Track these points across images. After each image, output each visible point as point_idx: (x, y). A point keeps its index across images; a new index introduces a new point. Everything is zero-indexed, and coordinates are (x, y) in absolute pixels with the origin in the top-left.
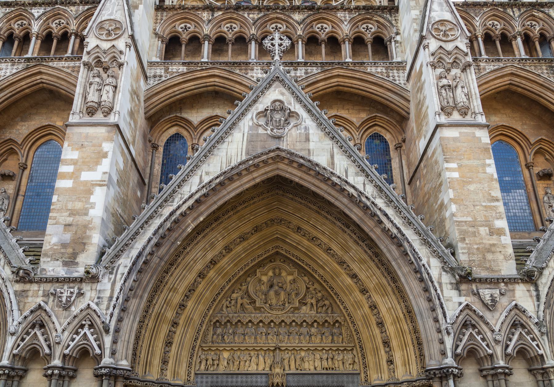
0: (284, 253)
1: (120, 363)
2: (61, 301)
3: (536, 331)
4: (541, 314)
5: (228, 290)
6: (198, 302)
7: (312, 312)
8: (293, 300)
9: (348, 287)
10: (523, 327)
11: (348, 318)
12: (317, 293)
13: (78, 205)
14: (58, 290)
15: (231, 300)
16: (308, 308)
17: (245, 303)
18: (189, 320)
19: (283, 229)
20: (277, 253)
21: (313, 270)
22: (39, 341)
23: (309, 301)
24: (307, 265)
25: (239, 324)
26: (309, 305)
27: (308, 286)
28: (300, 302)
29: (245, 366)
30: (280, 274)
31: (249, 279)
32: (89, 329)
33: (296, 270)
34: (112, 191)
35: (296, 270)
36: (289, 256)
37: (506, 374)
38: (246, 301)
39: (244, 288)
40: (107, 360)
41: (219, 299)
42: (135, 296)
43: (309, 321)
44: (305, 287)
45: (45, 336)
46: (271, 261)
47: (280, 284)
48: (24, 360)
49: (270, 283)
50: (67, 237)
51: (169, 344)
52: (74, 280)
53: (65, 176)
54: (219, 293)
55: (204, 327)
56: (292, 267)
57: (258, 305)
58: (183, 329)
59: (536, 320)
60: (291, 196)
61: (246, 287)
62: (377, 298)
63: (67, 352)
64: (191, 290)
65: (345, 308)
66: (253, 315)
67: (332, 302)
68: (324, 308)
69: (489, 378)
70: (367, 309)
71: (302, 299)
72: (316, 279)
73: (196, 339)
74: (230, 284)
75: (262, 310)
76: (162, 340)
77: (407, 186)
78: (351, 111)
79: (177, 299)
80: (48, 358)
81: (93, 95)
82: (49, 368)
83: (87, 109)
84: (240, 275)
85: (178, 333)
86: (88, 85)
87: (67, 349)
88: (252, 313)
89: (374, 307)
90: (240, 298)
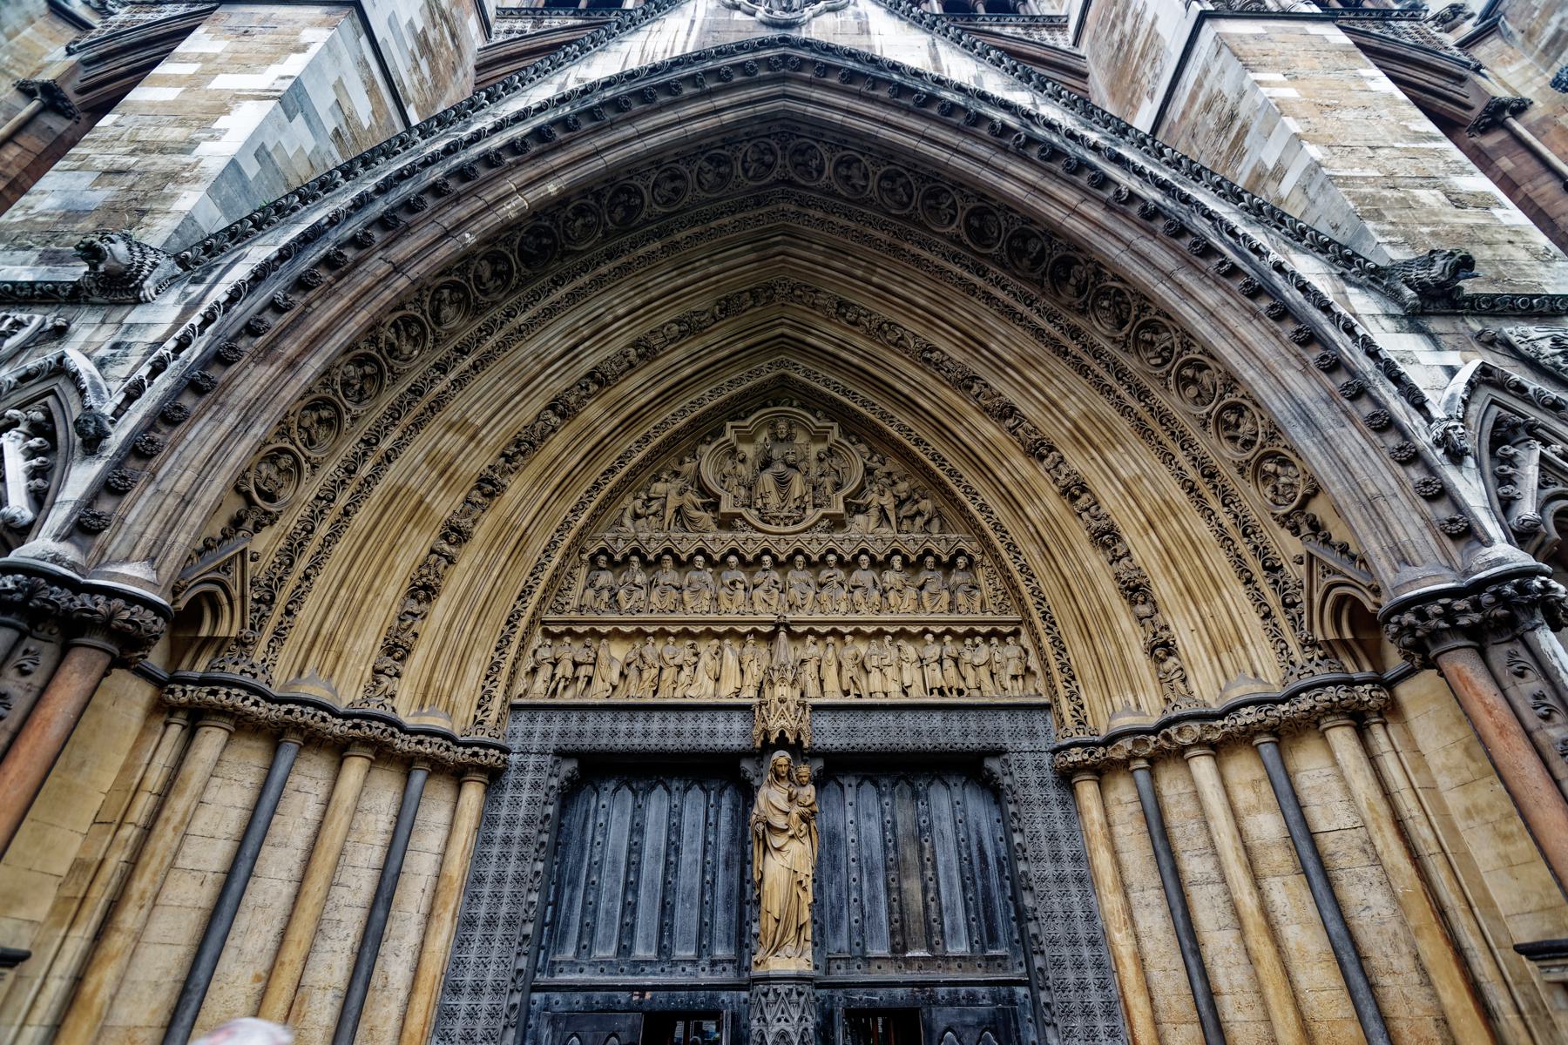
0: (800, 377)
7: (884, 530)
8: (829, 499)
12: (894, 483)
16: (873, 519)
19: (797, 312)
21: (883, 415)
26: (874, 512)
27: (870, 464)
28: (847, 505)
30: (790, 438)
33: (836, 425)
35: (836, 425)
38: (692, 497)
39: (689, 466)
46: (765, 406)
47: (791, 458)
49: (761, 458)
54: (612, 471)
57: (726, 507)
58: (482, 554)
60: (819, 214)
61: (694, 465)
66: (710, 536)
68: (919, 521)
70: (1054, 503)
75: (739, 523)
84: (677, 426)
85: (463, 564)
89: (1074, 490)
90: (674, 492)
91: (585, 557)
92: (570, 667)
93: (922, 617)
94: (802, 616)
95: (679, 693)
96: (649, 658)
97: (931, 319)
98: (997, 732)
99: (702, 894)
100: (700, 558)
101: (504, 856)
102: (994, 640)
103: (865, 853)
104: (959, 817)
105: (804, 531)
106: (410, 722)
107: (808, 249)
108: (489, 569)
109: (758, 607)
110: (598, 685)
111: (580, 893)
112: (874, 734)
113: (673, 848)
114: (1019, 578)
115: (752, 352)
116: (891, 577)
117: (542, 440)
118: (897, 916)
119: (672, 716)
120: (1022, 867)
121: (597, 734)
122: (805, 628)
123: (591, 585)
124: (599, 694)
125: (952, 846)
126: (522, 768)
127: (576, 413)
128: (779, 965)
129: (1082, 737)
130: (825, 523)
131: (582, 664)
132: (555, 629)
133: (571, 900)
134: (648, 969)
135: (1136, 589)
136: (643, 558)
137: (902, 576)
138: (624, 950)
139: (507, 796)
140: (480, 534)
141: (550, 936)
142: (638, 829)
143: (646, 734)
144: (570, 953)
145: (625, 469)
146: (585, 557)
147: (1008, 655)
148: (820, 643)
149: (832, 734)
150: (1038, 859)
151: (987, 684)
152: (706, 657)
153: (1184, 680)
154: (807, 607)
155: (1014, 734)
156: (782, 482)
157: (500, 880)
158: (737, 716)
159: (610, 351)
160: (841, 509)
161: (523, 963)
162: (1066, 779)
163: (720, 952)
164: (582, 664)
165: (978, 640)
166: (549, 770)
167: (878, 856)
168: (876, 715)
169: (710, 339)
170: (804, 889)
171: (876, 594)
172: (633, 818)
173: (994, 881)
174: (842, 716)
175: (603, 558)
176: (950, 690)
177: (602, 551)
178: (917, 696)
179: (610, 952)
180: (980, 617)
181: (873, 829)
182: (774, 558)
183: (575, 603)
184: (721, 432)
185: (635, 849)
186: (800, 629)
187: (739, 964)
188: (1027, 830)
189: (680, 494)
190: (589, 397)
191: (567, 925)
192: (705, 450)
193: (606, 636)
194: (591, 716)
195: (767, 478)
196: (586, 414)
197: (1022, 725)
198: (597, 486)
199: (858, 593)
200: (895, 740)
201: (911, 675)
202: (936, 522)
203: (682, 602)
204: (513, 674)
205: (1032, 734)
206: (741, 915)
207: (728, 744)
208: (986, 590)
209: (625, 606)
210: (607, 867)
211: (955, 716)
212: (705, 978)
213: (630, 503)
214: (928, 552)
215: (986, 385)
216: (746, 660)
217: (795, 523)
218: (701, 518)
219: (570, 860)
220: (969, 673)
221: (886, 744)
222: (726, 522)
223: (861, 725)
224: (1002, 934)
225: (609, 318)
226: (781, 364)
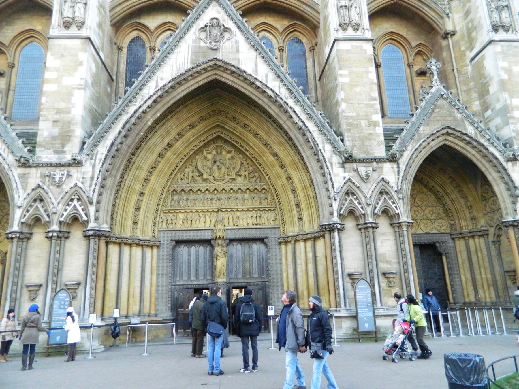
1: (102, 226)
2: (55, 181)
3: (396, 197)
4: (400, 184)
5: (182, 166)
6: (159, 176)
9: (271, 163)
10: (387, 194)
11: (271, 186)
13: (62, 105)
14: (52, 173)
16: (243, 179)
17: (195, 176)
18: (153, 190)
19: (222, 118)
20: (219, 137)
21: (246, 149)
22: (40, 211)
23: (243, 173)
24: (241, 145)
25: (191, 192)
26: (243, 177)
27: (243, 162)
28: (236, 175)
29: (195, 224)
30: (221, 153)
31: (197, 157)
32: (78, 202)
33: (233, 150)
34: (88, 92)
36: (227, 139)
37: (373, 228)
38: (196, 174)
39: (194, 164)
40: (92, 225)
41: (175, 173)
42: (110, 176)
43: (243, 188)
44: (240, 163)
45: (45, 208)
46: (214, 143)
47: (221, 161)
48: (30, 226)
50: (56, 131)
51: (138, 209)
52: (64, 165)
53: (49, 81)
54: (175, 169)
55: (164, 195)
56: (230, 147)
59: (396, 189)
61: (195, 163)
62: (292, 172)
63: (62, 219)
64: (154, 168)
65: (269, 178)
66: (201, 185)
68: (255, 179)
69: (363, 230)
70: (284, 180)
71: (238, 172)
72: (248, 156)
73: (158, 205)
74: (183, 161)
75: (208, 181)
76: (132, 206)
77: (317, 82)
78: (276, 19)
79: (143, 174)
80: (48, 224)
81: (68, 12)
82: (49, 232)
83: (64, 23)
85: (144, 200)
86: (63, 3)
87: (61, 217)
89: (289, 178)
90: (191, 173)
91: (170, 192)
93: (253, 207)
96: (189, 218)
97: (257, 126)
98: (267, 234)
100: (199, 192)
101: (163, 262)
106: (141, 238)
107: (223, 102)
108: (151, 201)
109: (214, 205)
112: (240, 235)
114: (276, 198)
116: (246, 196)
119: (196, 232)
123: (172, 200)
124: (178, 227)
125: (256, 257)
128: (219, 280)
129: (283, 236)
132: (166, 212)
135: (297, 205)
136: (185, 192)
138: (189, 278)
140: (146, 192)
142: (189, 255)
143: (190, 236)
144: (178, 279)
145: (178, 168)
147: (272, 215)
148: (229, 213)
149: (232, 235)
151: (266, 223)
152: (202, 218)
153: (302, 226)
155: (271, 234)
157: (163, 267)
158: (210, 231)
160: (234, 176)
161: (170, 281)
162: (280, 243)
163: (208, 278)
167: (241, 259)
169: (198, 128)
173: (264, 263)
174: (233, 230)
175: (175, 192)
177: (174, 190)
178: (251, 226)
179: (186, 278)
180: (266, 206)
181: (240, 254)
182: (218, 191)
183: (169, 205)
185: (189, 259)
187: (212, 280)
191: (177, 274)
194: (177, 232)
195: (215, 168)
198: (171, 174)
199: (238, 201)
201: (249, 221)
202: (259, 179)
203: (195, 204)
205: (275, 234)
206: (212, 271)
208: (269, 199)
210: (184, 263)
211: (258, 230)
212: (206, 282)
214: (256, 189)
216: (211, 218)
219: (176, 262)
220: (263, 220)
224: (265, 273)
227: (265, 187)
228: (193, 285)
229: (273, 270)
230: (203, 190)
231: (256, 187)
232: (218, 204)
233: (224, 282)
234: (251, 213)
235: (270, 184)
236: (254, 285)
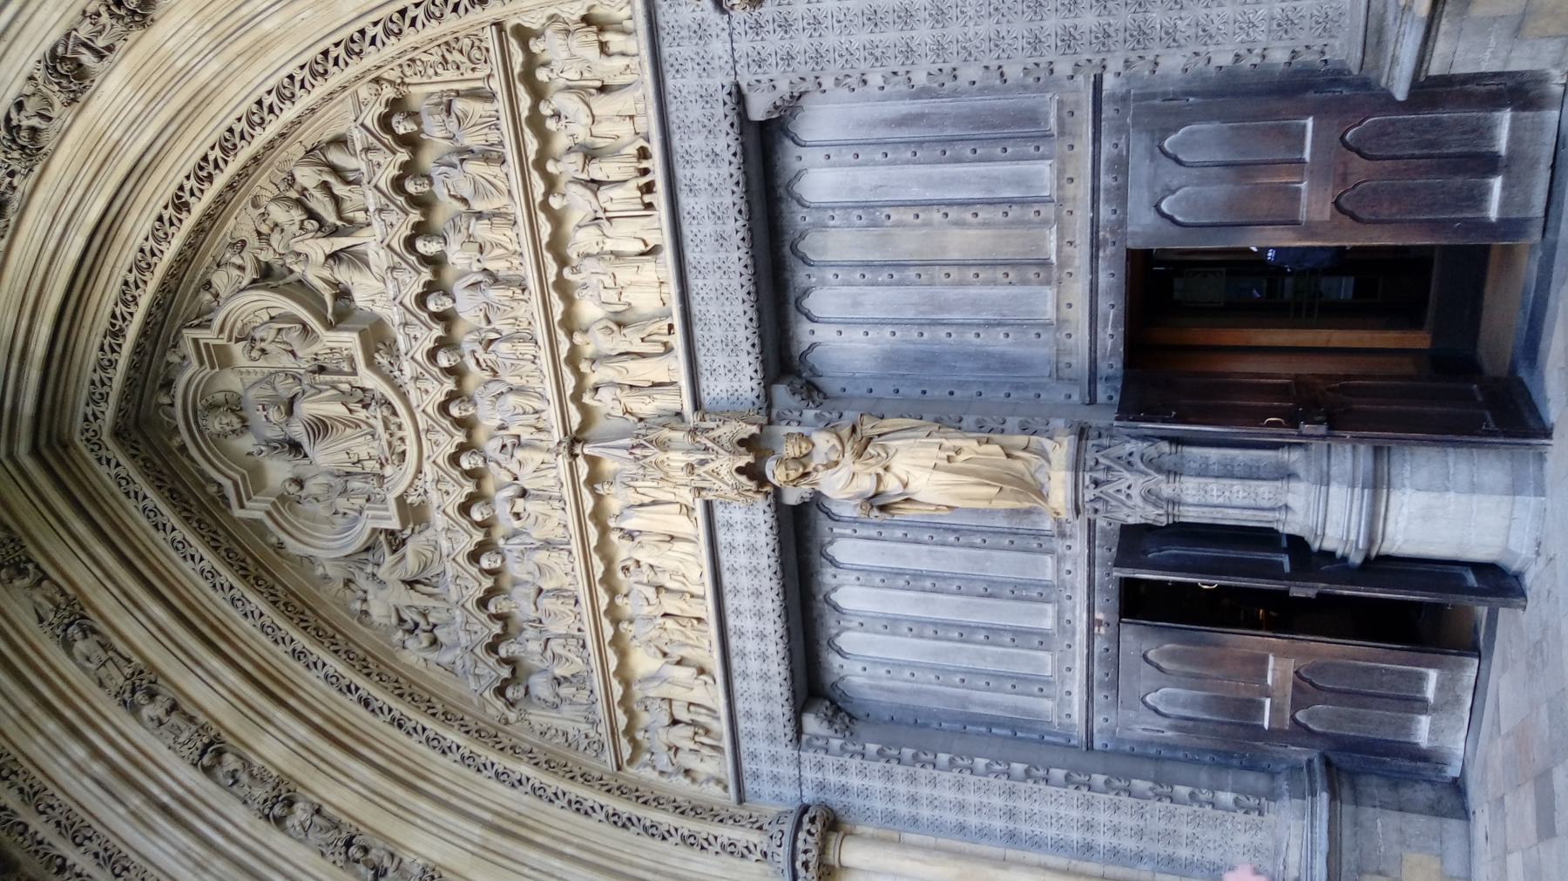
0: (109, 411)
7: (372, 258)
15: (401, 621)
17: (400, 573)
26: (343, 275)
27: (250, 275)
35: (189, 334)
44: (253, 295)
54: (366, 703)
67: (297, 151)
68: (339, 189)
71: (318, 310)
74: (318, 652)
84: (264, 608)
88: (436, 546)
90: (383, 594)
91: (512, 716)
92: (677, 729)
93: (520, 212)
94: (552, 414)
95: (698, 590)
98: (706, 98)
99: (973, 546)
102: (542, 75)
103: (910, 314)
104: (850, 157)
105: (404, 397)
110: (699, 694)
111: (976, 695)
113: (913, 579)
115: (86, 499)
116: (458, 257)
117: (337, 826)
118: (999, 273)
119: (730, 602)
120: (920, 78)
121: (768, 698)
122: (572, 409)
125: (896, 171)
126: (822, 786)
127: (283, 779)
130: (382, 359)
131: (672, 715)
133: (984, 705)
134: (1068, 616)
137: (451, 237)
138: (1043, 640)
139: (858, 802)
141: (1030, 730)
142: (890, 624)
143: (762, 636)
145: (359, 680)
146: (512, 716)
148: (593, 379)
150: (908, 52)
152: (641, 555)
154: (538, 405)
156: (320, 428)
158: (720, 514)
159: (157, 747)
160: (348, 341)
161: (1058, 774)
164: (672, 715)
165: (545, 109)
166: (821, 754)
168: (696, 307)
169: (83, 577)
170: (958, 451)
171: (495, 294)
172: (876, 632)
173: (947, 105)
175: (509, 693)
176: (645, 172)
177: (500, 691)
178: (657, 229)
179: (1045, 656)
180: (501, 104)
183: (585, 727)
184: (256, 525)
185: (917, 627)
186: (575, 419)
188: (863, 66)
189: (382, 583)
190: (247, 764)
191: (1016, 709)
192: (293, 546)
193: (627, 683)
194: (740, 706)
196: (279, 761)
197: (688, 49)
200: (736, 281)
201: (625, 237)
202: (336, 157)
204: (695, 810)
207: (765, 528)
209: (577, 665)
211: (682, 172)
212: (1079, 546)
213: (414, 654)
215: (20, 106)
217: (395, 413)
218: (418, 553)
221: (742, 294)
222: (414, 514)
223: (718, 333)
225: (98, 768)
226: (95, 443)
227: (371, 117)
228: (1092, 623)
229: (996, 41)
230: (468, 540)
231: (384, 184)
232: (538, 457)
233: (1077, 466)
234: (575, 218)
235: (321, 88)
236: (1121, 195)
